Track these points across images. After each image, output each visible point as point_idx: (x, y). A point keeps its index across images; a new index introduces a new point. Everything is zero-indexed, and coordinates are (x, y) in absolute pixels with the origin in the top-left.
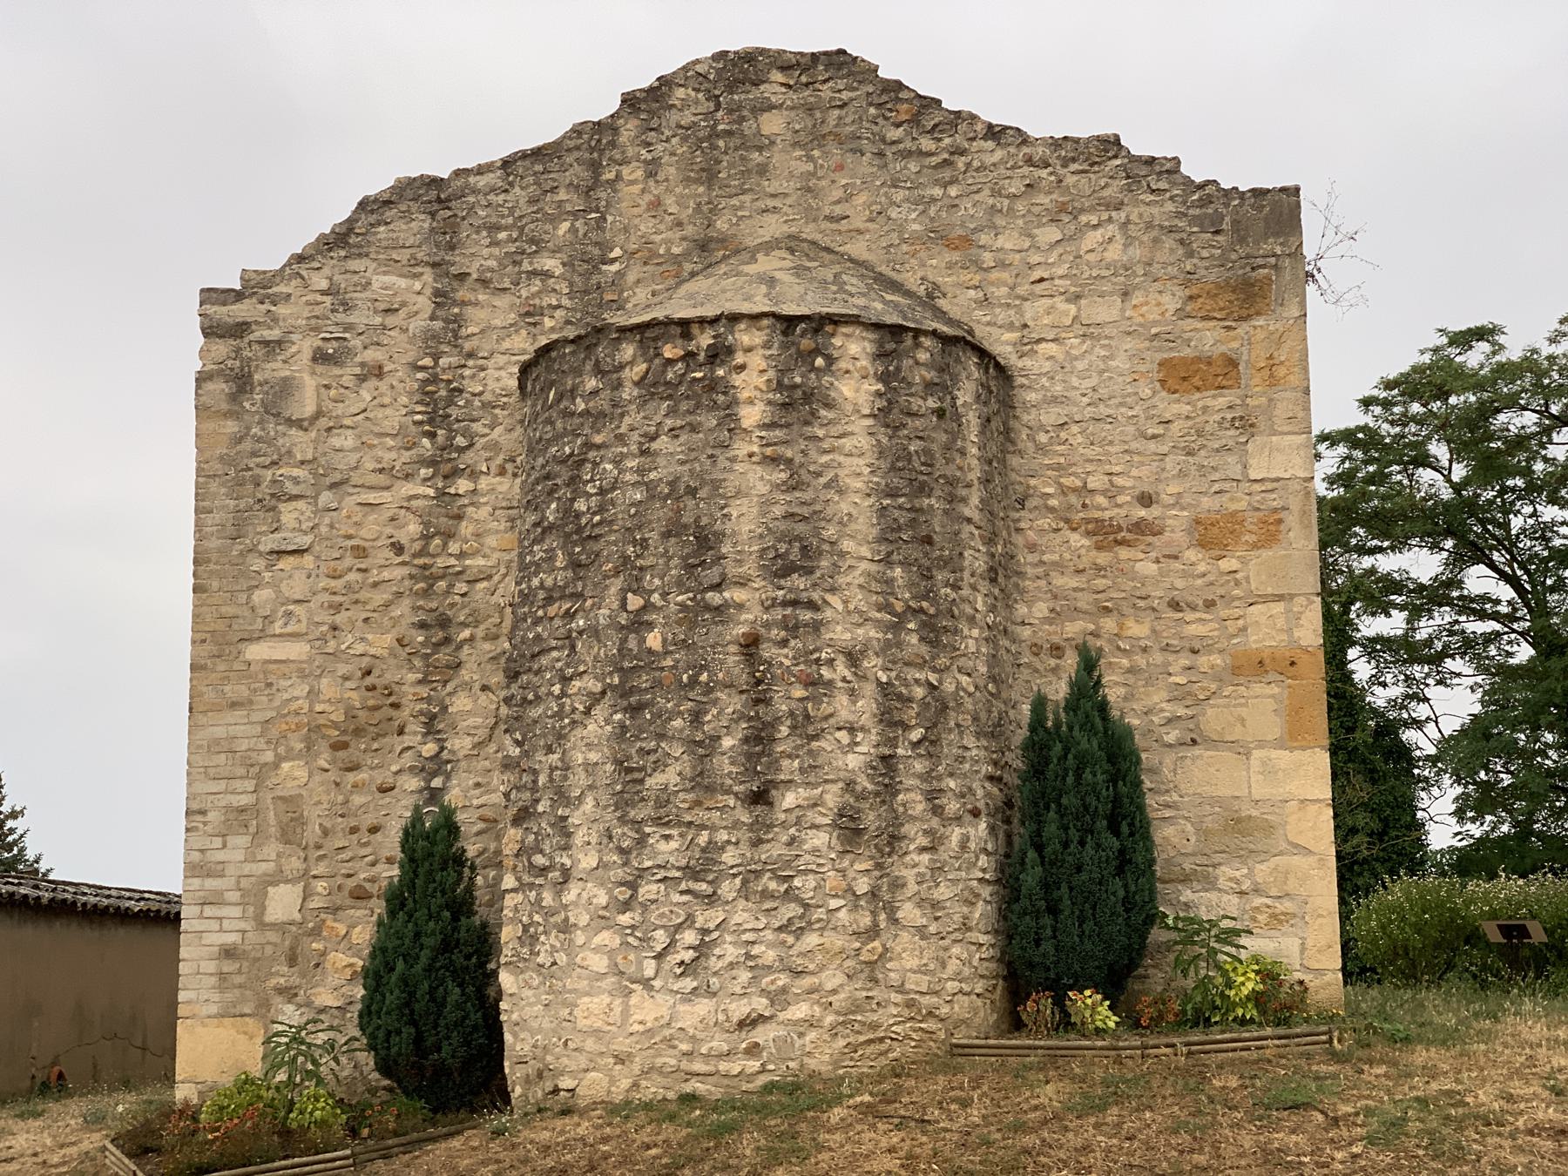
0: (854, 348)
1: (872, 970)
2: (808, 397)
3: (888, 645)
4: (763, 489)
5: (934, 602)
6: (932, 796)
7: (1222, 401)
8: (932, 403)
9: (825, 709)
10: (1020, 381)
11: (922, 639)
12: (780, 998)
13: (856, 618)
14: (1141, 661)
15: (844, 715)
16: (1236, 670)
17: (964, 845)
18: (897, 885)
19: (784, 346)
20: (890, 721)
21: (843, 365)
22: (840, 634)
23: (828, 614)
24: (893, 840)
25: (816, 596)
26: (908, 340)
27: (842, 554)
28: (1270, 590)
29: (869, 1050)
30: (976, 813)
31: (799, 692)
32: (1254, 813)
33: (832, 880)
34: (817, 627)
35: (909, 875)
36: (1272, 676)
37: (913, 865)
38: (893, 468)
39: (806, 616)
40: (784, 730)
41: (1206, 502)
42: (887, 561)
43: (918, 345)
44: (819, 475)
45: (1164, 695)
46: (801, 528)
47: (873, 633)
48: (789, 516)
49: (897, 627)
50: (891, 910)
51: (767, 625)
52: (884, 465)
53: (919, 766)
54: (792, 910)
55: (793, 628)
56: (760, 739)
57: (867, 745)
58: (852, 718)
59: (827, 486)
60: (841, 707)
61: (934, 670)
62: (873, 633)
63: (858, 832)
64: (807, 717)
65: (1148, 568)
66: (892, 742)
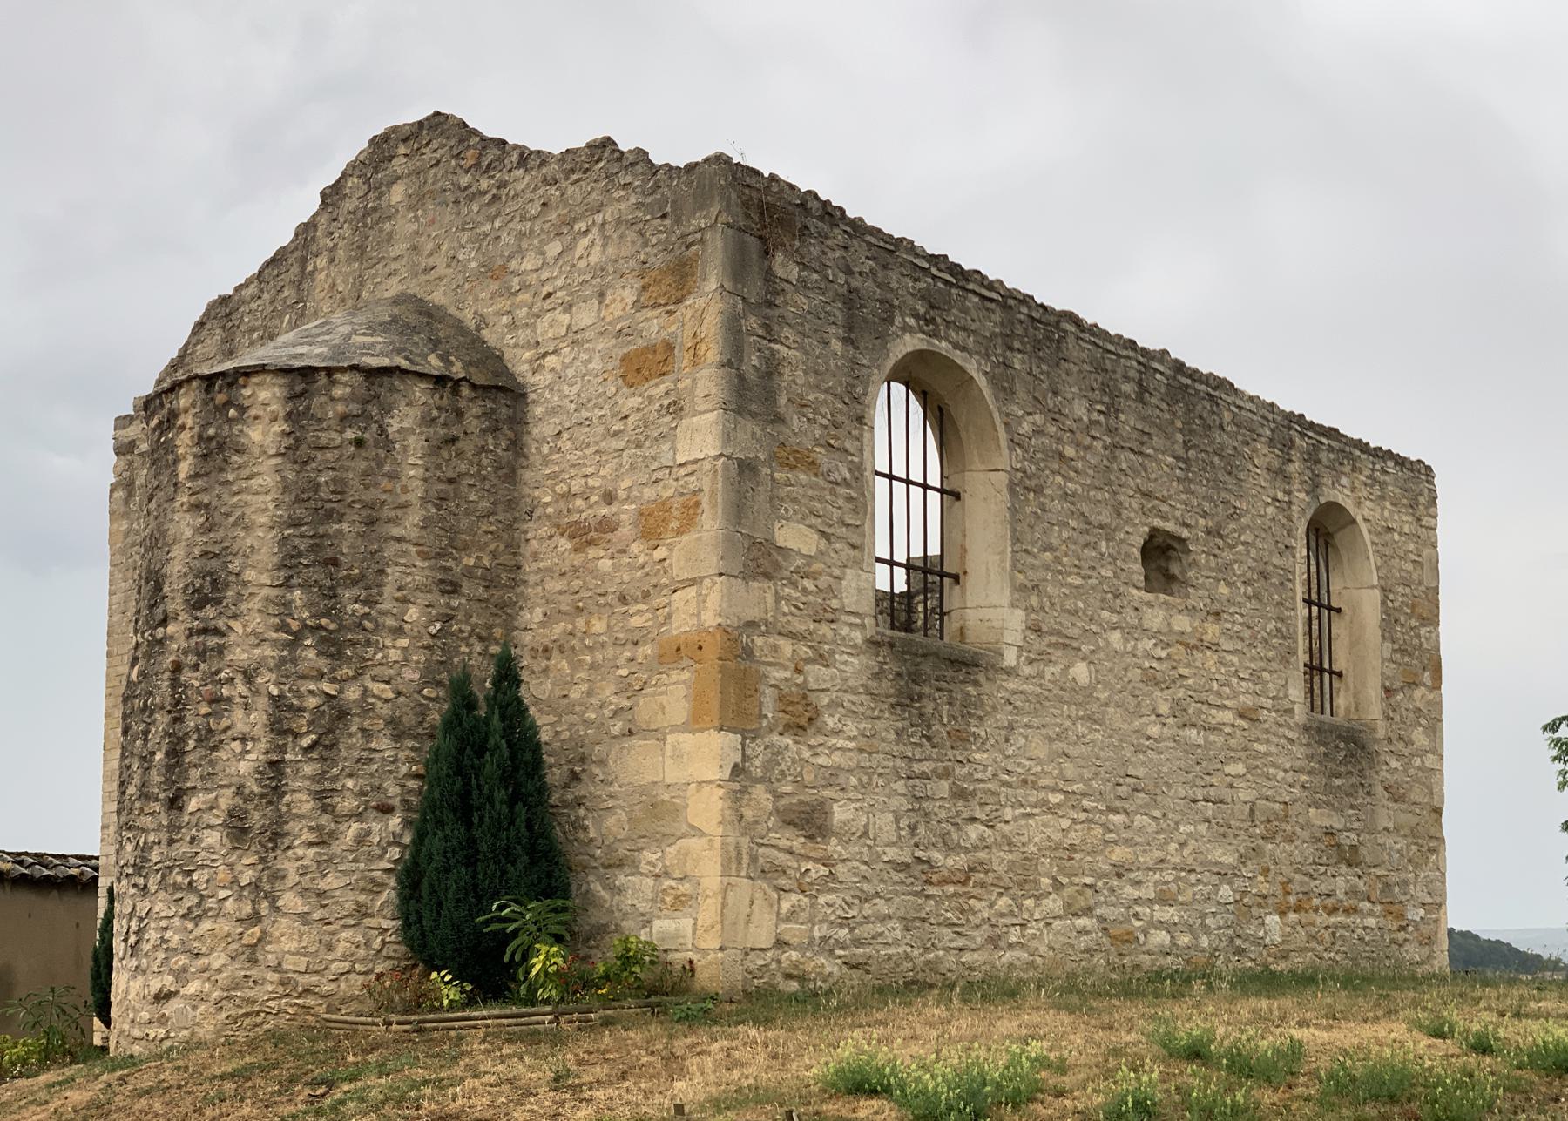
0: (264, 395)
1: (252, 954)
2: (221, 447)
4: (188, 533)
5: (337, 618)
6: (323, 797)
7: (663, 388)
8: (350, 434)
9: (225, 723)
11: (320, 654)
12: (181, 975)
13: (253, 640)
14: (599, 656)
15: (240, 727)
16: (661, 658)
17: (361, 840)
19: (205, 403)
20: (280, 729)
21: (253, 412)
22: (239, 655)
23: (232, 638)
24: (275, 837)
25: (221, 624)
26: (323, 379)
27: (245, 584)
28: (686, 576)
29: (247, 1021)
30: (386, 810)
31: (204, 709)
32: (666, 797)
33: (223, 874)
34: (220, 650)
35: (291, 868)
36: (686, 662)
37: (297, 857)
38: (297, 500)
39: (213, 641)
40: (191, 743)
41: (648, 493)
42: (287, 585)
43: (334, 383)
44: (228, 515)
45: (612, 688)
47: (268, 652)
48: (204, 554)
49: (293, 645)
50: (273, 900)
51: (185, 653)
52: (288, 498)
53: (308, 769)
54: (191, 900)
55: (202, 653)
56: (176, 753)
57: (257, 754)
58: (246, 729)
59: (235, 524)
60: (238, 720)
61: (333, 680)
62: (268, 652)
63: (245, 831)
64: (210, 731)
65: (606, 565)
66: (282, 749)
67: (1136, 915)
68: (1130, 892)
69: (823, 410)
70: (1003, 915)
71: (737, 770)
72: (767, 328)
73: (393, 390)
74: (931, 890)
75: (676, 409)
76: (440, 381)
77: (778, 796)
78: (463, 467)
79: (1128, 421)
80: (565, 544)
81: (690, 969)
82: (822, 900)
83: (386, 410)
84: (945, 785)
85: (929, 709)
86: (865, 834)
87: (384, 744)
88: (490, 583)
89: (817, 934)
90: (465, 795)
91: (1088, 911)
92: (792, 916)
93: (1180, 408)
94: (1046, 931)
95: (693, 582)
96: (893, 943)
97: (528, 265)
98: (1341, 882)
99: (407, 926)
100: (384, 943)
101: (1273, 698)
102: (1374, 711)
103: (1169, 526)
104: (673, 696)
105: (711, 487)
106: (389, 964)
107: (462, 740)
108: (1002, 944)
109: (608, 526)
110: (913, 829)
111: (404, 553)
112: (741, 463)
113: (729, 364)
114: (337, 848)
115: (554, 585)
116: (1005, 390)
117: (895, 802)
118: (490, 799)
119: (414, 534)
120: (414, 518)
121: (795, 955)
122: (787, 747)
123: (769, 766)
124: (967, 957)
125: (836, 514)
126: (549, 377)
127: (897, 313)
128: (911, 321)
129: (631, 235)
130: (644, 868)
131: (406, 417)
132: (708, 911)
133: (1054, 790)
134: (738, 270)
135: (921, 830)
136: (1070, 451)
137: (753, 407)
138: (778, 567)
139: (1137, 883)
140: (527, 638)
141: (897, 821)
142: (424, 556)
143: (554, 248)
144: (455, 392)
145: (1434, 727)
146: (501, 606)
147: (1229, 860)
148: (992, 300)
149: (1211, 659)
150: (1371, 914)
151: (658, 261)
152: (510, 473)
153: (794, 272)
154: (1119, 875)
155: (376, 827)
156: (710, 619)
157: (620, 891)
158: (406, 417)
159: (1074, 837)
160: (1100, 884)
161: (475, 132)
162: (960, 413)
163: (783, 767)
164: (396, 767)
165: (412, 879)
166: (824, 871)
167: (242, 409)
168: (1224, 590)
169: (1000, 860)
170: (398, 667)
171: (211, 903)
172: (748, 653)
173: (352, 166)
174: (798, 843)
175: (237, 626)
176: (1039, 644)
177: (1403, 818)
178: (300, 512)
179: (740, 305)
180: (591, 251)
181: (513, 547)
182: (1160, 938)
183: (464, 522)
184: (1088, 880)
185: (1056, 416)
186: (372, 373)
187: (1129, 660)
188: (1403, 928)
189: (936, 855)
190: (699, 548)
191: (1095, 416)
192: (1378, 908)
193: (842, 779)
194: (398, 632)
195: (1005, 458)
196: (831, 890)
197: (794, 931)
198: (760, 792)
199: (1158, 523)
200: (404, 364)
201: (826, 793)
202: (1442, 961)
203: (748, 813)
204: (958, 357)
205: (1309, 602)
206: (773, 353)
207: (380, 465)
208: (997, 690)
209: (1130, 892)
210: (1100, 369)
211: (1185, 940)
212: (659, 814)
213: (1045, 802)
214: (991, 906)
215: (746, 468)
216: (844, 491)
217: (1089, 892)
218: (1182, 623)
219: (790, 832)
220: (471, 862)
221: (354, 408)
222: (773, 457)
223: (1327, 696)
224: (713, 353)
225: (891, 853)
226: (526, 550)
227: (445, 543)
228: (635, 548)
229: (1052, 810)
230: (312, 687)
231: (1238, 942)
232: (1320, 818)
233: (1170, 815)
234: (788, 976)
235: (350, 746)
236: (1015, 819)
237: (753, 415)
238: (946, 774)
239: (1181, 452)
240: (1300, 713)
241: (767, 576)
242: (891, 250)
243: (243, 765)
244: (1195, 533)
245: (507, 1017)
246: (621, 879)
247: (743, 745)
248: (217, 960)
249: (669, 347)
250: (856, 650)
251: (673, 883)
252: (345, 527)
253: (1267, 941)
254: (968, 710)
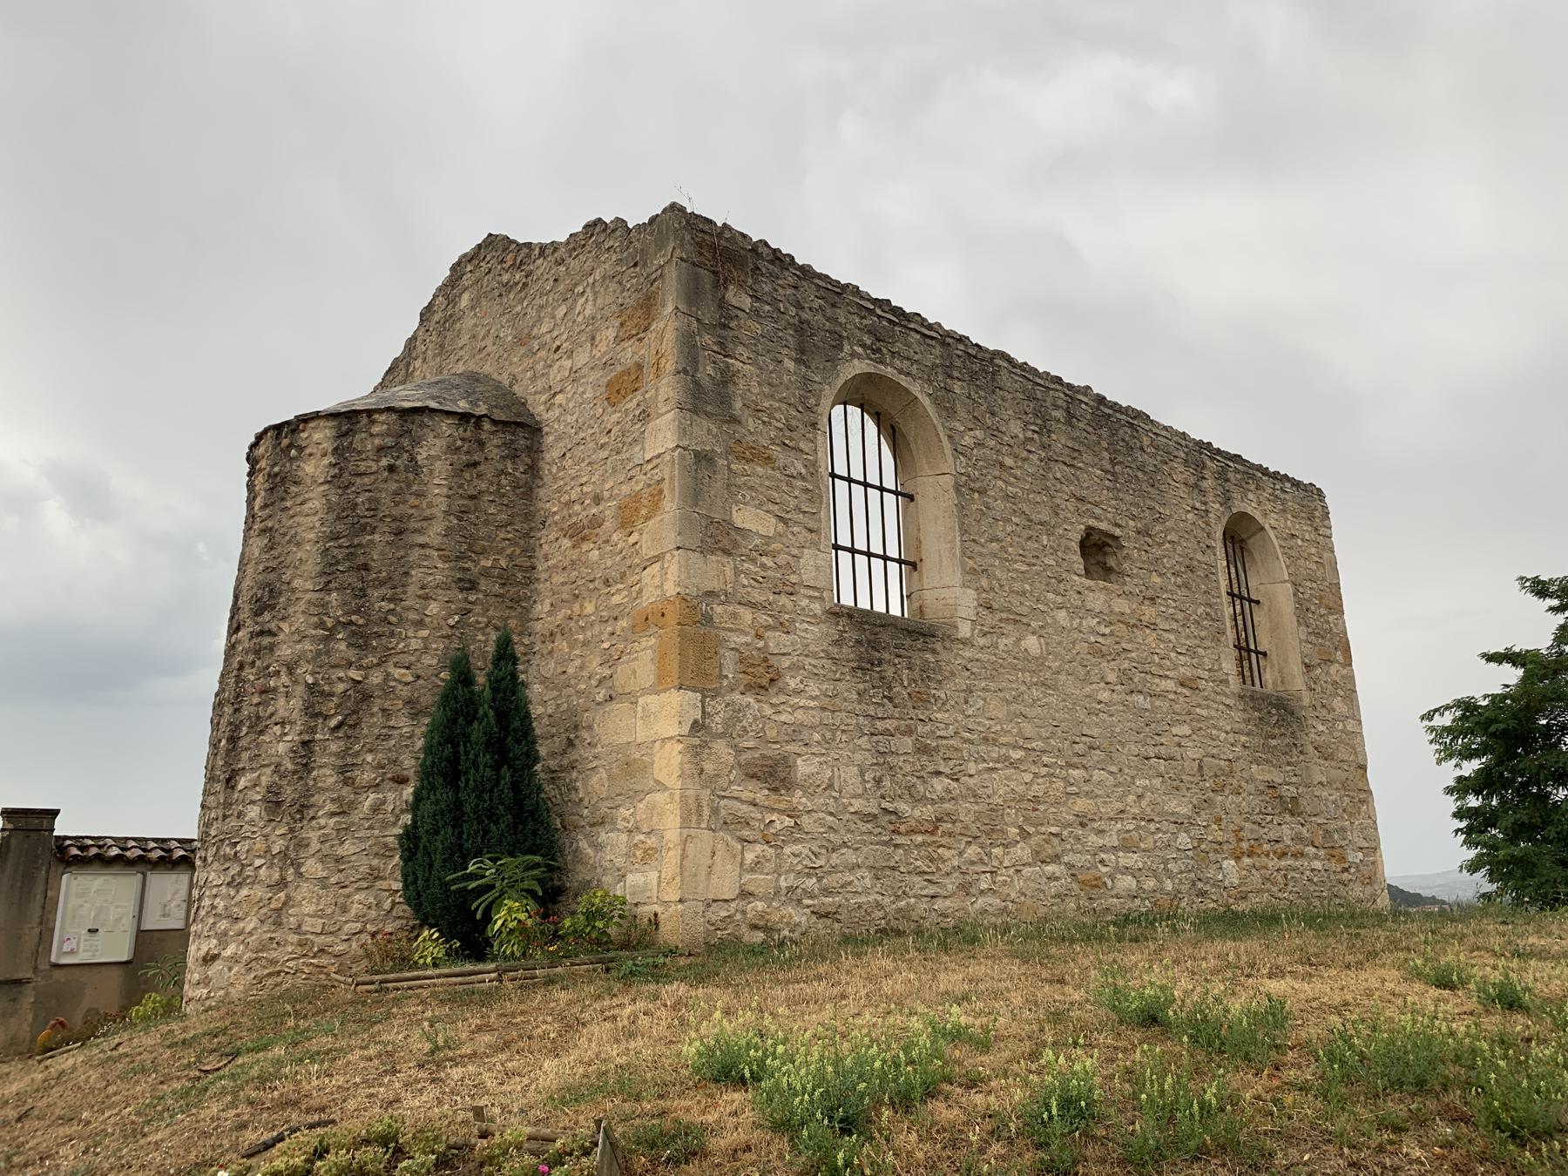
0: (317, 436)
1: (277, 917)
2: (283, 480)
3: (319, 653)
5: (366, 615)
6: (345, 772)
8: (384, 462)
9: (271, 709)
10: (546, 429)
11: (350, 645)
13: (296, 637)
15: (282, 713)
17: (376, 809)
18: (303, 845)
21: (308, 451)
22: (285, 652)
23: (281, 636)
24: (303, 809)
25: (273, 626)
26: (364, 420)
27: (293, 591)
28: (652, 553)
29: (271, 981)
30: (401, 781)
31: (256, 700)
32: (637, 755)
34: (272, 648)
35: (314, 836)
36: (653, 629)
38: (338, 518)
39: (266, 641)
41: (625, 489)
42: (326, 589)
43: (373, 422)
44: (285, 535)
45: (598, 660)
46: (273, 576)
47: (308, 647)
49: (326, 639)
50: (297, 865)
52: (331, 517)
58: (286, 714)
59: (289, 542)
60: (282, 707)
61: (360, 668)
62: (308, 647)
63: (279, 804)
64: (258, 718)
66: (313, 730)
67: (1102, 861)
68: (1094, 840)
69: (777, 415)
70: (973, 863)
71: (696, 726)
72: (721, 345)
73: (422, 425)
74: (899, 840)
75: (644, 416)
76: (464, 417)
77: (739, 751)
78: (484, 486)
79: (1060, 440)
80: (567, 543)
81: (655, 921)
82: (787, 850)
83: (416, 442)
84: (909, 741)
85: (890, 672)
86: (830, 786)
87: (403, 723)
88: (506, 579)
89: (783, 884)
90: (454, 761)
91: (1056, 858)
92: (756, 866)
93: (1104, 432)
94: (1018, 879)
95: (658, 558)
96: (863, 891)
97: (544, 329)
98: (1287, 831)
99: (406, 887)
100: (394, 904)
101: (1209, 670)
102: (1298, 683)
103: (1103, 526)
104: (642, 664)
105: (671, 474)
106: (398, 923)
107: (456, 711)
108: (973, 891)
109: (596, 522)
110: (878, 782)
111: (427, 557)
112: (697, 455)
113: (685, 371)
114: (355, 817)
115: (558, 579)
116: (948, 411)
117: (858, 757)
118: (475, 765)
119: (436, 541)
120: (438, 527)
121: (760, 905)
122: (748, 705)
123: (728, 723)
124: (939, 904)
125: (793, 503)
126: (557, 412)
127: (845, 342)
128: (860, 350)
129: (613, 286)
130: (621, 824)
131: (433, 447)
132: (671, 860)
133: (1015, 747)
134: (692, 295)
135: (887, 783)
136: (1009, 462)
137: (709, 408)
138: (736, 545)
139: (1100, 832)
140: (538, 626)
141: (862, 774)
142: (446, 559)
143: (562, 310)
144: (478, 426)
145: (1351, 696)
146: (517, 600)
147: (1185, 810)
148: (932, 338)
149: (1151, 638)
150: (1316, 857)
151: (630, 300)
152: (527, 491)
153: (746, 302)
154: (1083, 825)
155: (391, 796)
156: (671, 589)
157: (598, 847)
158: (433, 447)
159: (1037, 789)
160: (1065, 833)
161: (514, 242)
162: (909, 428)
163: (744, 723)
164: (407, 739)
165: (411, 842)
166: (789, 822)
167: (301, 449)
168: (1156, 579)
169: (966, 811)
170: (418, 658)
171: (249, 871)
172: (708, 619)
173: (439, 289)
174: (761, 795)
175: (285, 626)
176: (991, 620)
177: (1334, 773)
178: (340, 527)
179: (695, 324)
180: (586, 307)
181: (529, 552)
182: (1127, 882)
183: (483, 532)
184: (1054, 830)
185: (995, 432)
186: (405, 413)
187: (1075, 635)
188: (1345, 870)
189: (902, 806)
190: (662, 529)
191: (1029, 434)
192: (1322, 852)
193: (805, 735)
194: (420, 624)
195: (949, 463)
196: (797, 841)
197: (759, 881)
198: (720, 746)
199: (1092, 522)
200: (433, 405)
201: (790, 748)
202: (1384, 901)
203: (709, 767)
204: (903, 381)
205: (1231, 594)
206: (728, 366)
207: (409, 486)
208: (953, 659)
209: (1094, 840)
210: (1031, 398)
211: (1150, 884)
212: (632, 767)
213: (1007, 758)
214: (961, 854)
215: (703, 459)
216: (799, 483)
217: (1056, 841)
218: (1121, 605)
219: (752, 785)
220: (457, 823)
221: (389, 441)
222: (729, 451)
223: (1256, 674)
224: (669, 364)
225: (857, 805)
226: (540, 554)
227: (465, 546)
228: (615, 537)
229: (1014, 765)
230: (341, 674)
231: (1200, 885)
232: (1262, 773)
233: (1126, 770)
234: (755, 927)
235: (372, 723)
236: (979, 773)
237: (709, 415)
238: (909, 732)
239: (1108, 467)
240: (1234, 684)
241: (727, 553)
242: (839, 293)
243: (280, 746)
244: (1126, 532)
245: (457, 975)
246: (603, 837)
247: (703, 702)
248: (250, 924)
249: (639, 367)
250: (815, 620)
251: (642, 837)
252: (377, 537)
254: (927, 674)
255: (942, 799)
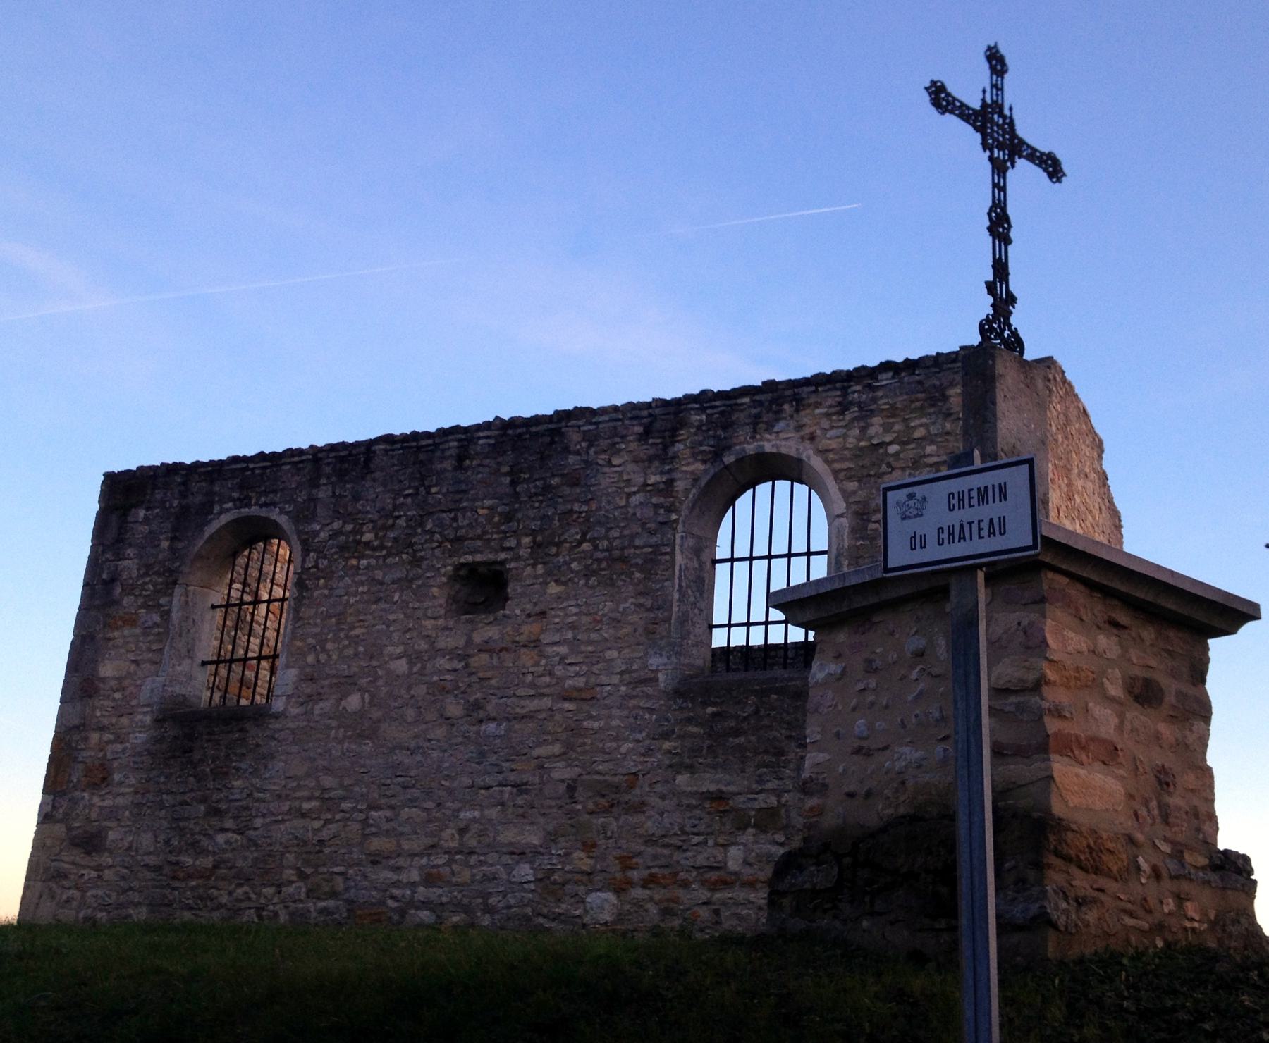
67: (392, 897)
70: (241, 901)
82: (89, 894)
86: (129, 848)
139: (397, 869)
154: (374, 863)
166: (94, 874)
184: (336, 870)
214: (230, 893)
253: (587, 920)
255: (224, 851)
